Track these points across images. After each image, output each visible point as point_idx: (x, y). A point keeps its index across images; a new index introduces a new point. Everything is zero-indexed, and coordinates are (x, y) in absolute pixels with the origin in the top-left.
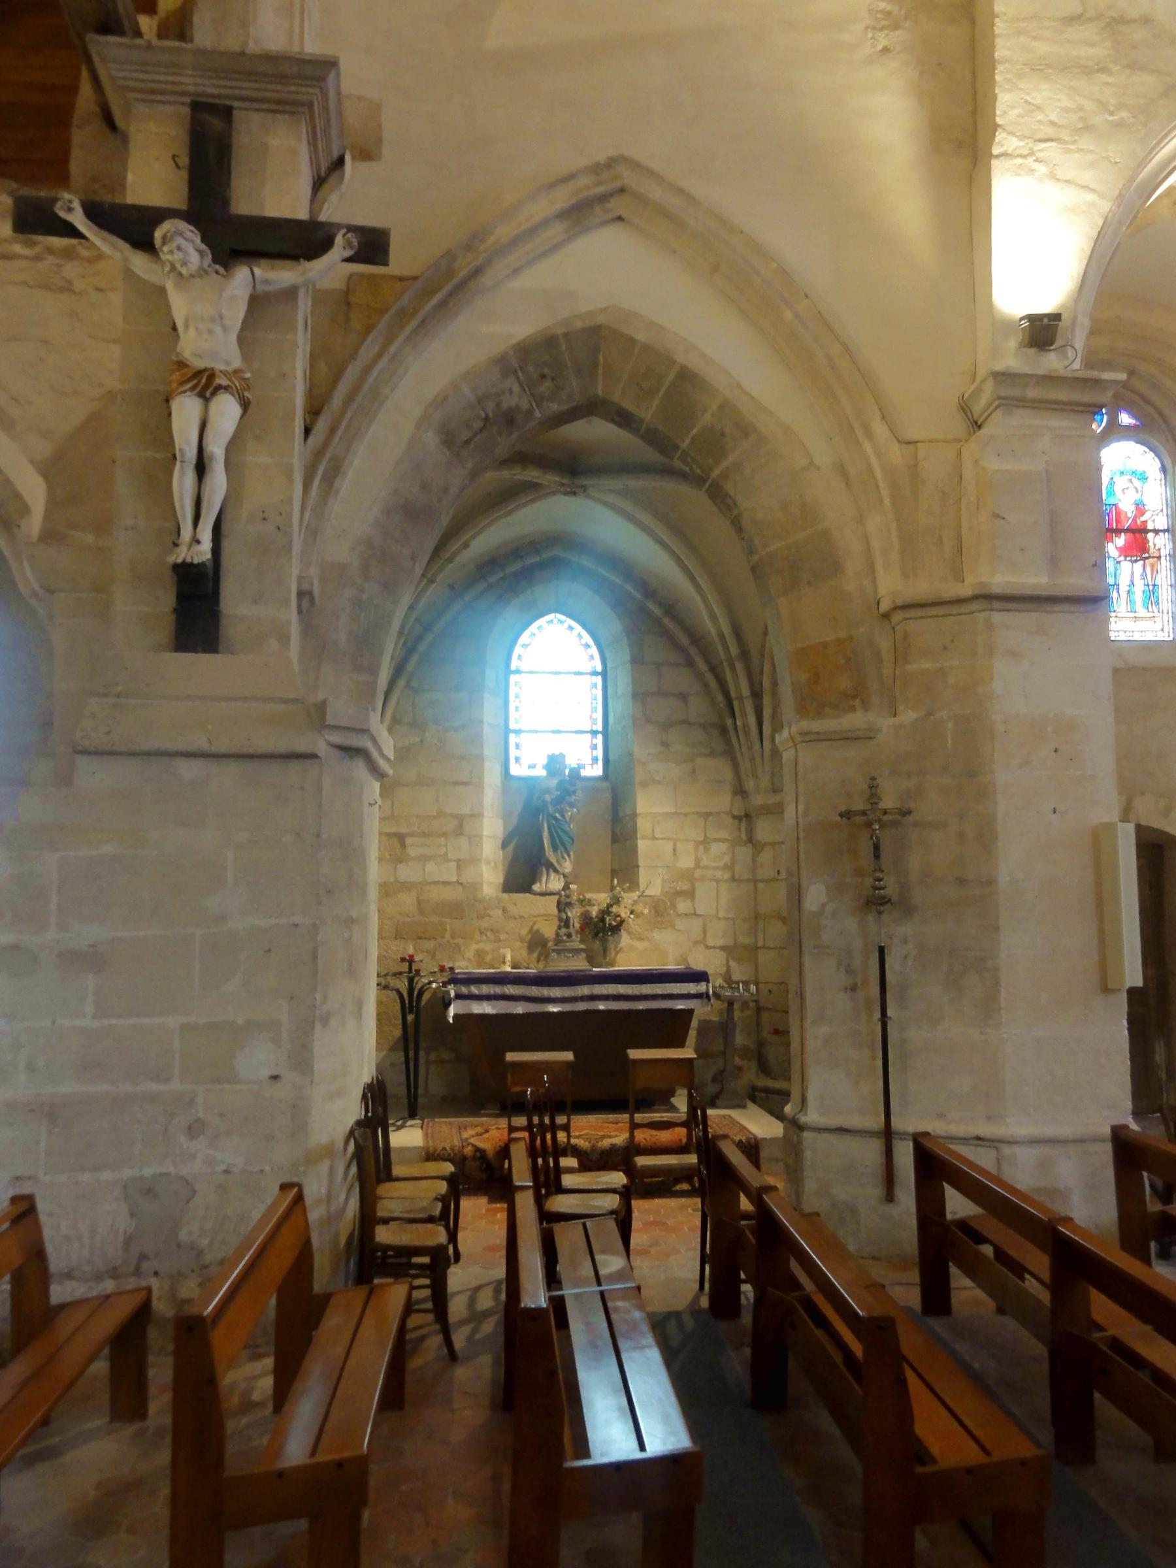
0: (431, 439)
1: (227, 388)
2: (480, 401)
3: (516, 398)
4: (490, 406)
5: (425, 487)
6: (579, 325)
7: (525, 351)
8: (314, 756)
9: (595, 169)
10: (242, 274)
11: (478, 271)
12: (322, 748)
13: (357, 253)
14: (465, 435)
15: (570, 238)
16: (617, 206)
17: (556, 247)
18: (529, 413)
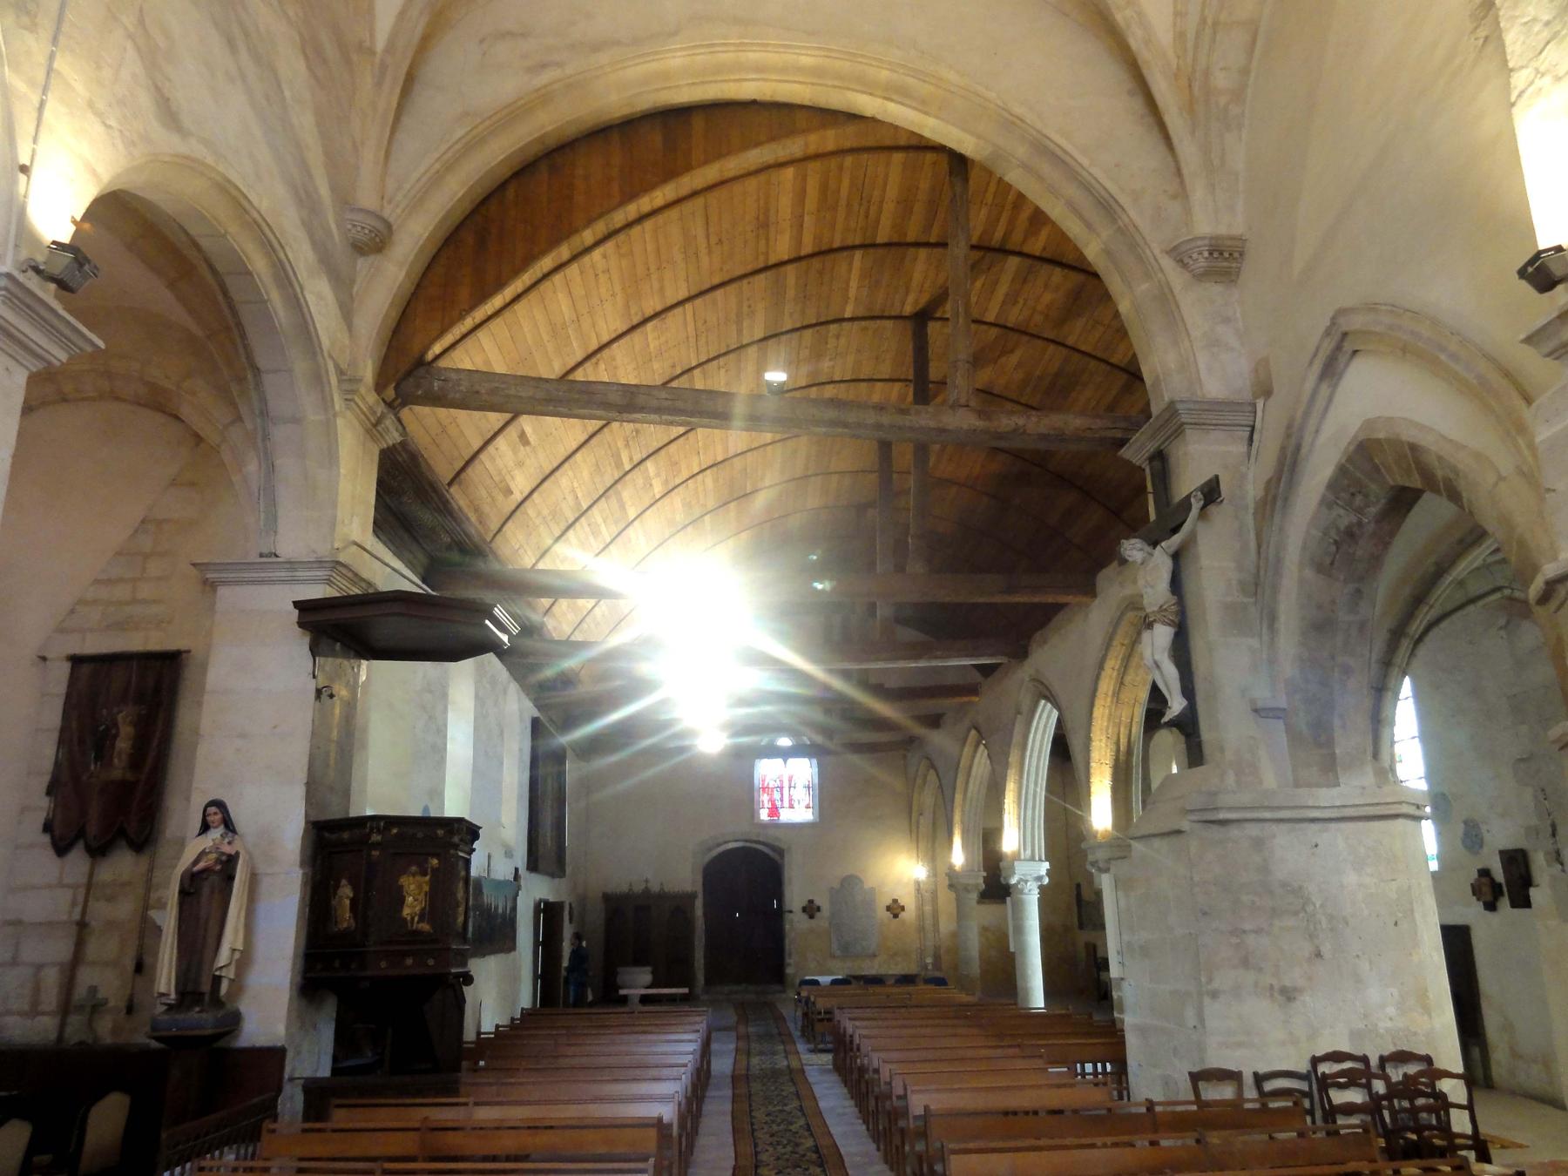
0: (1309, 573)
1: (1155, 621)
2: (1325, 534)
3: (1346, 519)
4: (1333, 533)
5: (1320, 607)
6: (1352, 448)
7: (1333, 486)
8: (1179, 832)
9: (1328, 333)
10: (1158, 547)
11: (1298, 448)
12: (1185, 825)
13: (1205, 500)
14: (1328, 561)
15: (1334, 387)
16: (1348, 346)
17: (1330, 400)
18: (1360, 524)
